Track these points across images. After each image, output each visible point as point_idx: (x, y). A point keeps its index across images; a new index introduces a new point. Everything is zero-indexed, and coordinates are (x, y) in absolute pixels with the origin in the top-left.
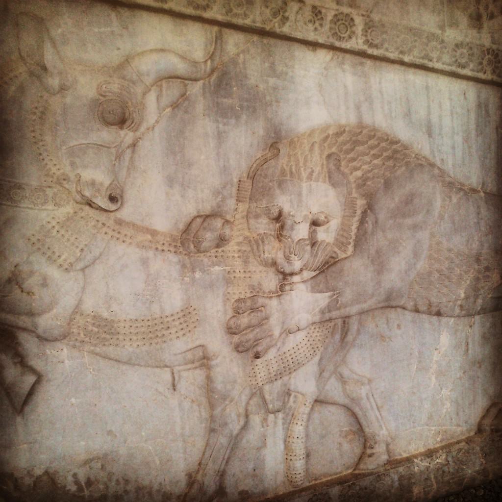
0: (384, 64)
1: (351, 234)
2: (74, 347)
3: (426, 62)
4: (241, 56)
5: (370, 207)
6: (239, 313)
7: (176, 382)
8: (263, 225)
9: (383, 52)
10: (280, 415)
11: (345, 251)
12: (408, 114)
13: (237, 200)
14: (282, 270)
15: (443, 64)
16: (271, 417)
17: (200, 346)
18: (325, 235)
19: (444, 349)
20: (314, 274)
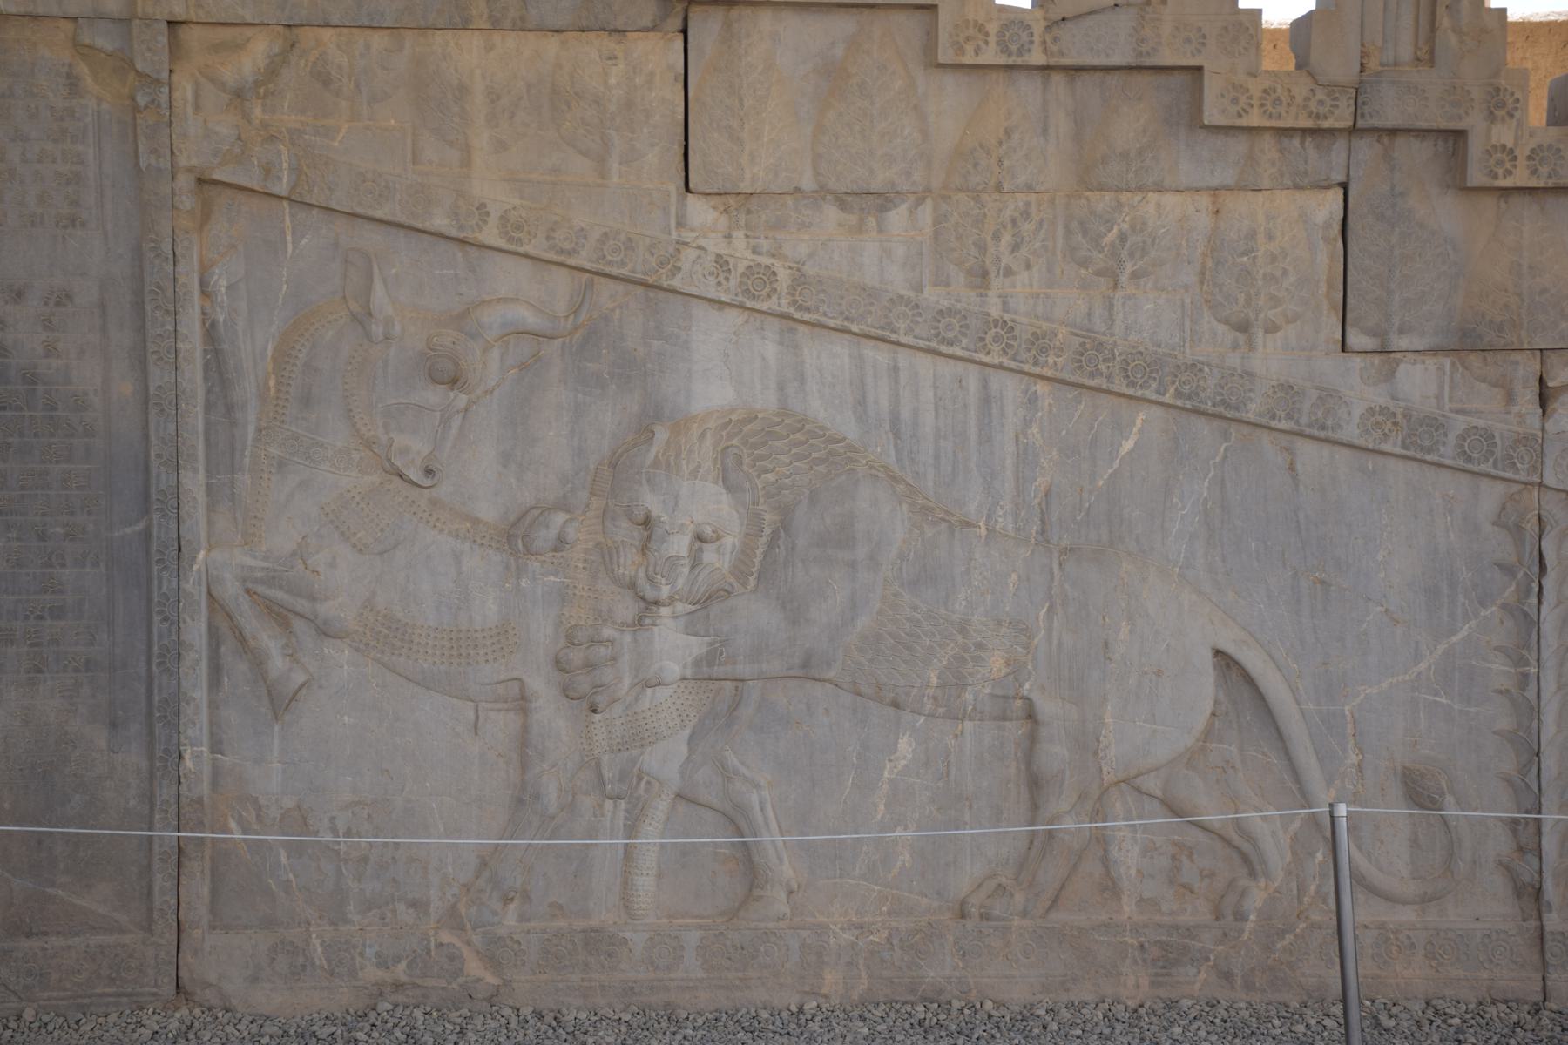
0: (825, 332)
1: (754, 560)
2: (357, 650)
3: (887, 333)
4: (618, 311)
5: (785, 525)
6: (574, 644)
7: (480, 724)
8: (625, 531)
9: (819, 318)
10: (623, 804)
11: (744, 585)
12: (861, 402)
13: (591, 493)
14: (642, 594)
15: (915, 337)
16: (609, 804)
17: (516, 679)
18: (718, 560)
19: (903, 763)
20: (693, 608)
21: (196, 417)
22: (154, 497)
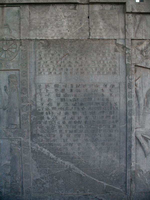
21: (134, 107)
22: (128, 120)
